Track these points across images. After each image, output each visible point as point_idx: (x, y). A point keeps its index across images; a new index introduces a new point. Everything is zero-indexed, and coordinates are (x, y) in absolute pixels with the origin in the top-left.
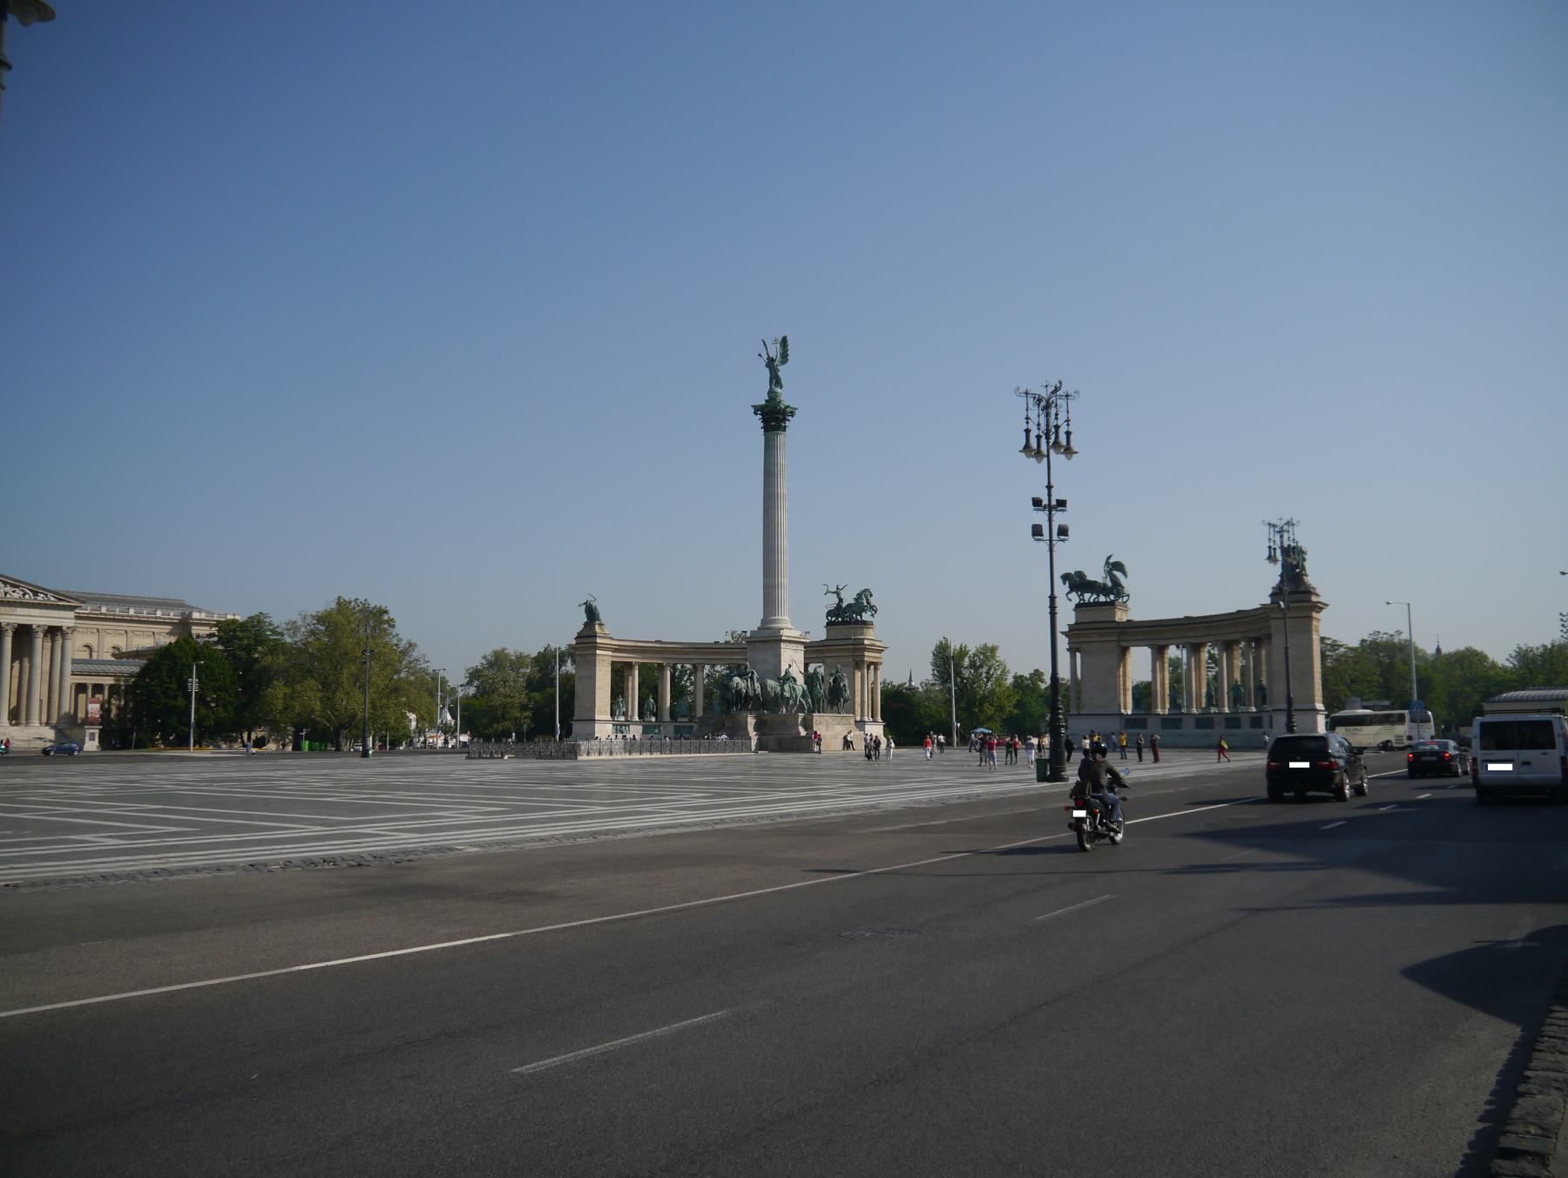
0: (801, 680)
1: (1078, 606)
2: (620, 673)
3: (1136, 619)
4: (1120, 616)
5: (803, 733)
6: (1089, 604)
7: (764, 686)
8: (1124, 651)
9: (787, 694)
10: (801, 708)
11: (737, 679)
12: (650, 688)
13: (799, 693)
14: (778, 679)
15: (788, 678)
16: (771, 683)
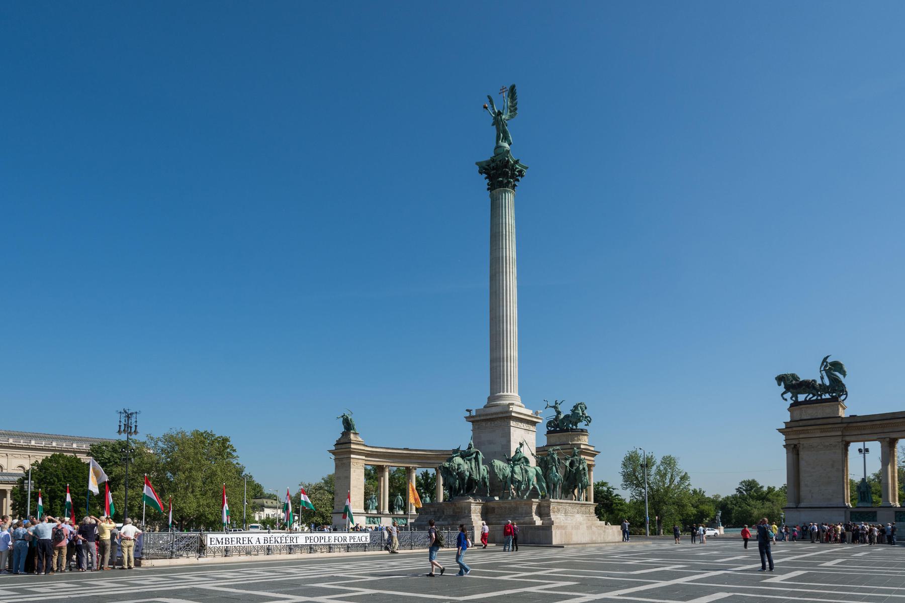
0: (533, 462)
1: (792, 405)
2: (373, 475)
3: (859, 413)
4: (843, 413)
5: (538, 522)
6: (806, 402)
7: (492, 472)
8: (847, 444)
9: (518, 477)
10: (534, 494)
11: (458, 460)
12: (398, 489)
13: (532, 473)
14: (508, 461)
15: (518, 460)
16: (498, 463)
